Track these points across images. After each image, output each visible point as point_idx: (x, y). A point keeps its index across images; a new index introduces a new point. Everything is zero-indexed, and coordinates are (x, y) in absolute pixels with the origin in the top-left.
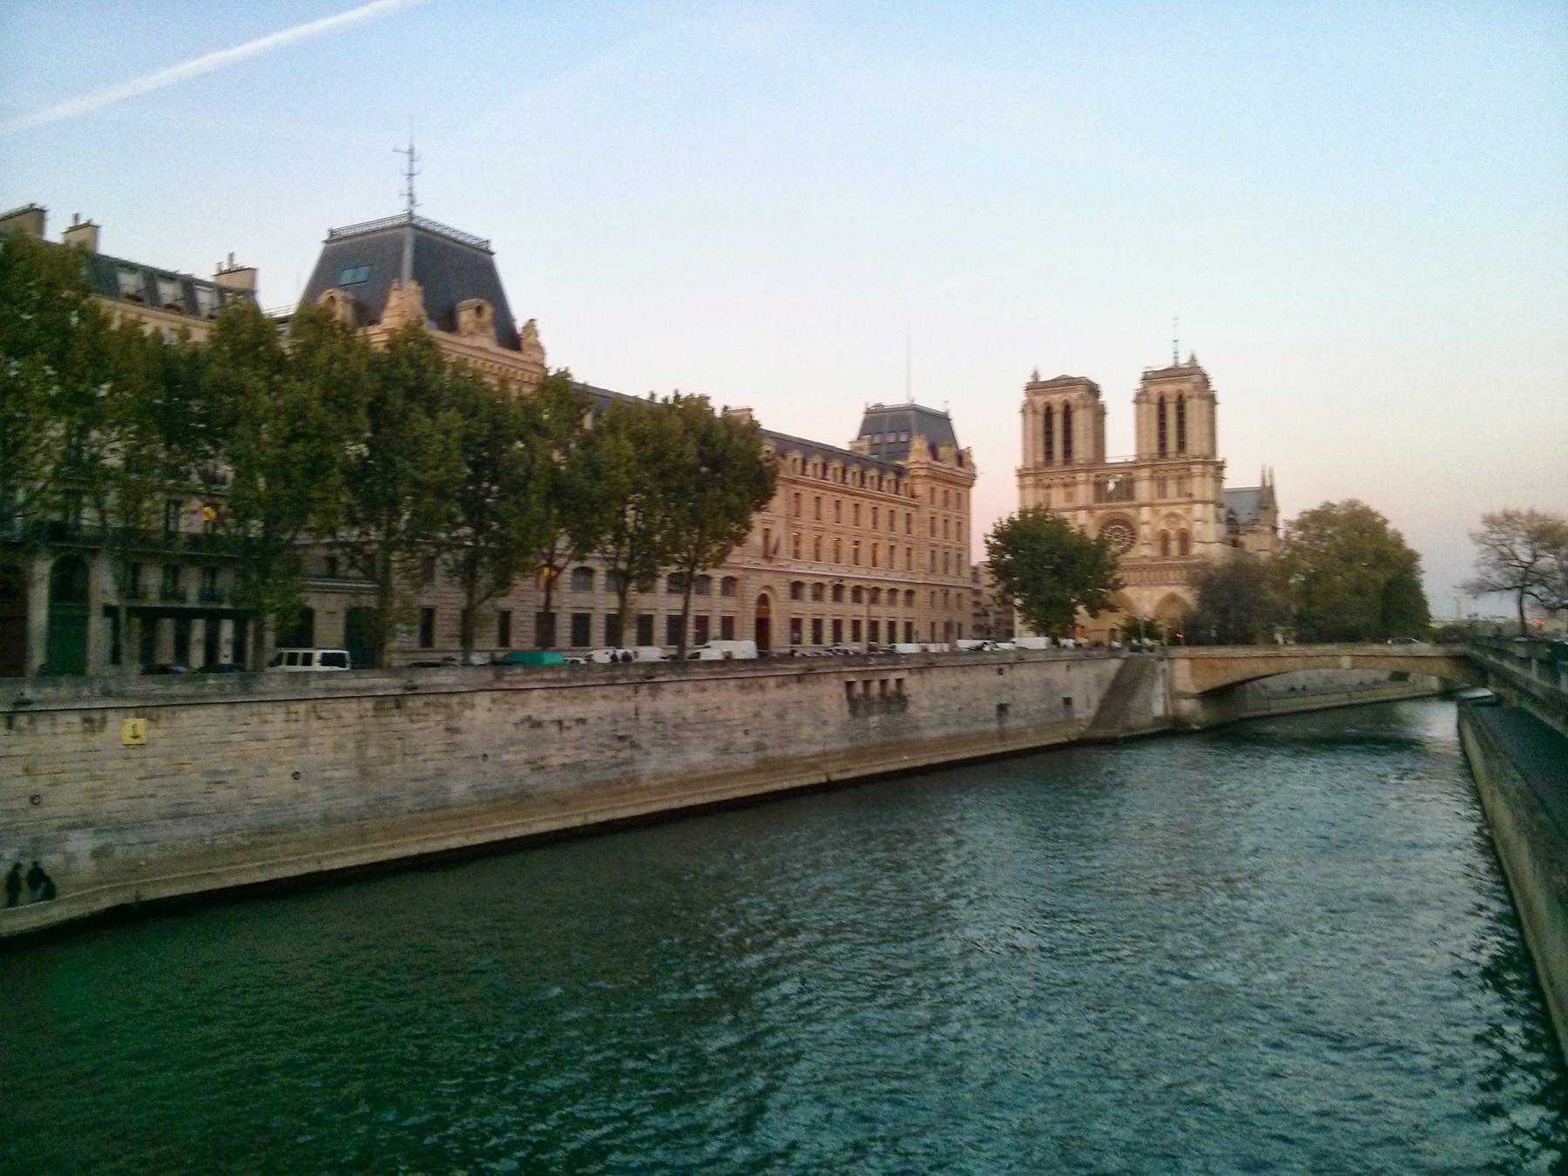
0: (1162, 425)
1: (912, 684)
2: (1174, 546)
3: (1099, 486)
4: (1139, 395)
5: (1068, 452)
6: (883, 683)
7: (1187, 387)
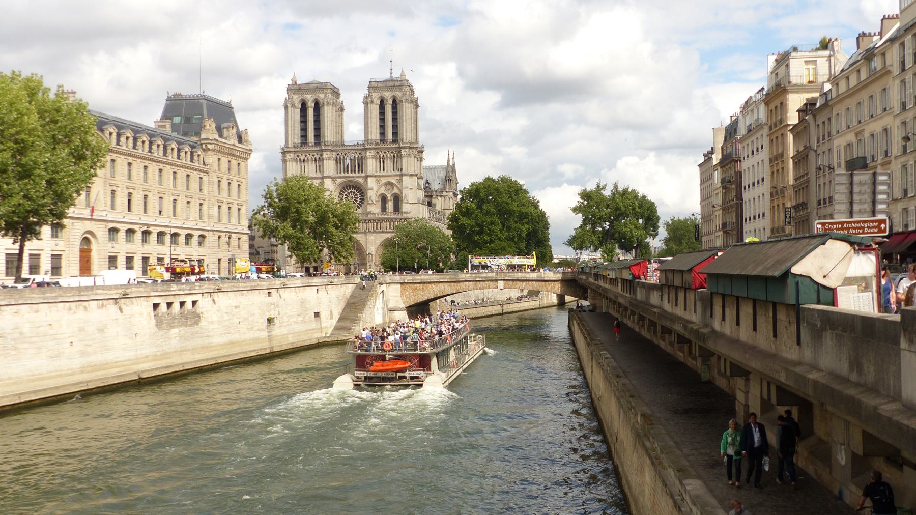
0: (383, 120)
1: (204, 303)
2: (390, 206)
3: (338, 161)
4: (366, 98)
5: (318, 136)
6: (182, 304)
7: (398, 94)
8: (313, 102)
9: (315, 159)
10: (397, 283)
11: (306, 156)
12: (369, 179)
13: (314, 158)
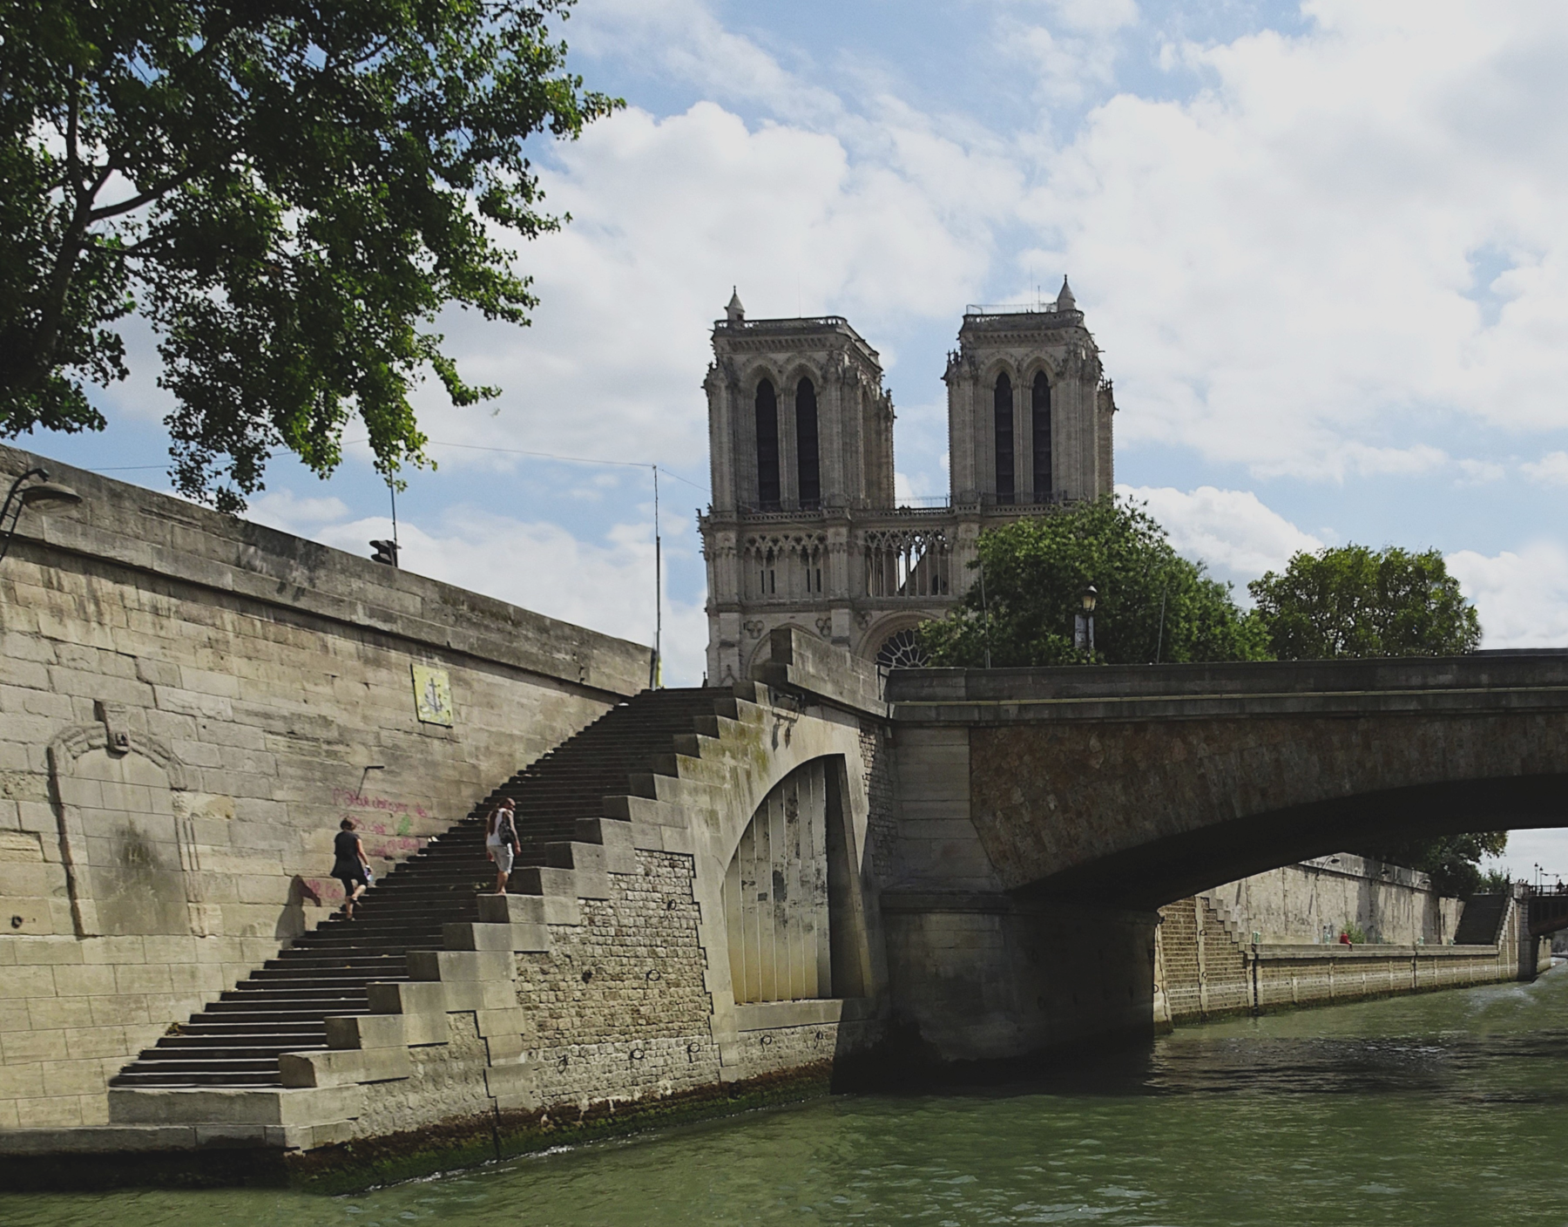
9: (804, 549)
11: (775, 541)
13: (799, 548)
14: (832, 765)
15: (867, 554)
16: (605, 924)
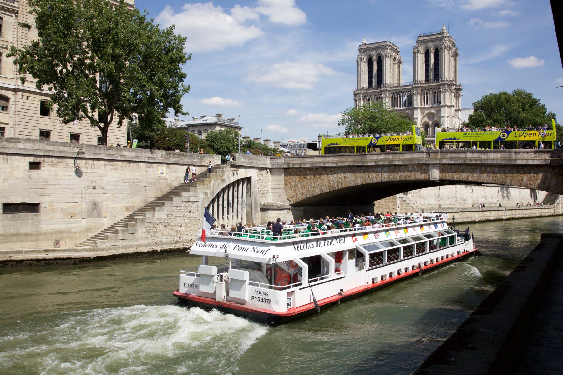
8: (376, 57)
10: (280, 168)
11: (370, 96)
12: (415, 112)
14: (249, 179)
15: (392, 98)
16: (172, 216)
